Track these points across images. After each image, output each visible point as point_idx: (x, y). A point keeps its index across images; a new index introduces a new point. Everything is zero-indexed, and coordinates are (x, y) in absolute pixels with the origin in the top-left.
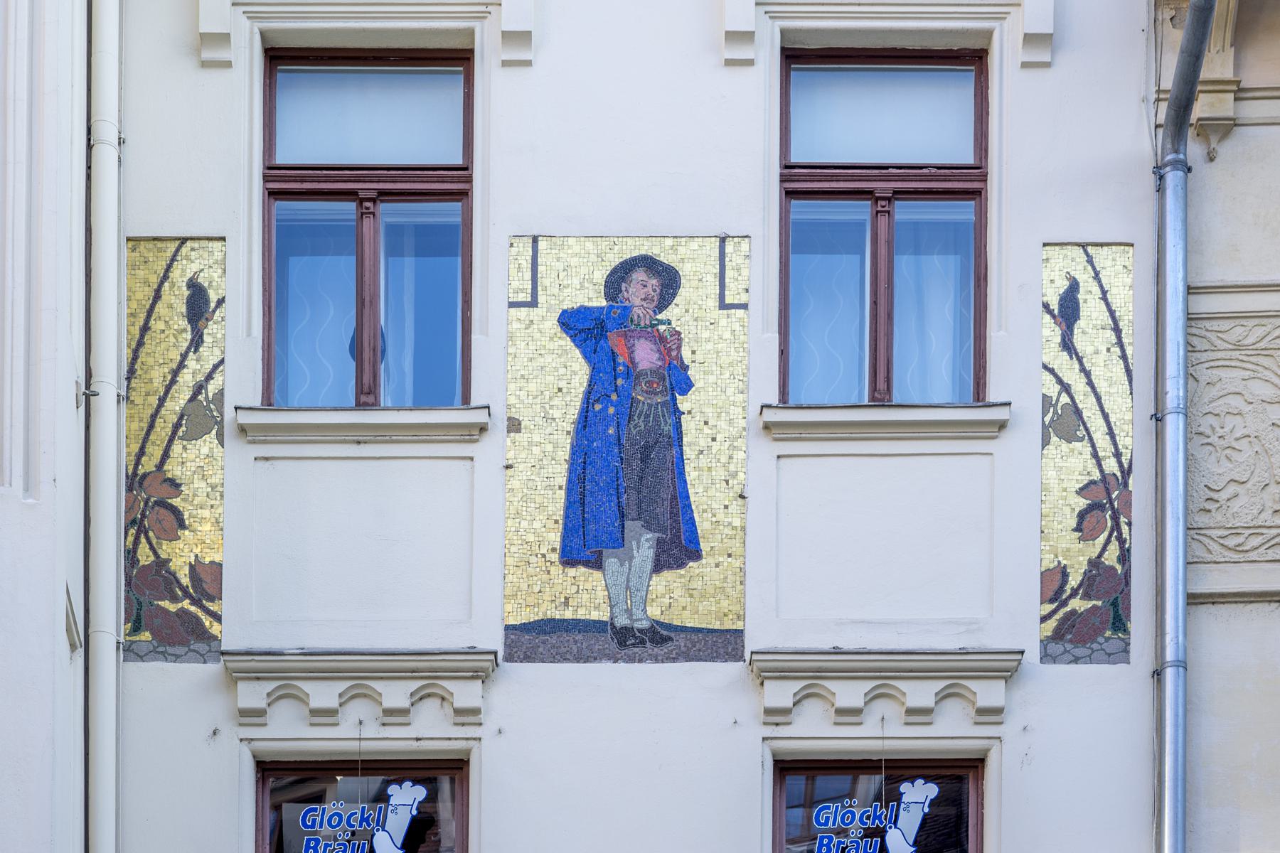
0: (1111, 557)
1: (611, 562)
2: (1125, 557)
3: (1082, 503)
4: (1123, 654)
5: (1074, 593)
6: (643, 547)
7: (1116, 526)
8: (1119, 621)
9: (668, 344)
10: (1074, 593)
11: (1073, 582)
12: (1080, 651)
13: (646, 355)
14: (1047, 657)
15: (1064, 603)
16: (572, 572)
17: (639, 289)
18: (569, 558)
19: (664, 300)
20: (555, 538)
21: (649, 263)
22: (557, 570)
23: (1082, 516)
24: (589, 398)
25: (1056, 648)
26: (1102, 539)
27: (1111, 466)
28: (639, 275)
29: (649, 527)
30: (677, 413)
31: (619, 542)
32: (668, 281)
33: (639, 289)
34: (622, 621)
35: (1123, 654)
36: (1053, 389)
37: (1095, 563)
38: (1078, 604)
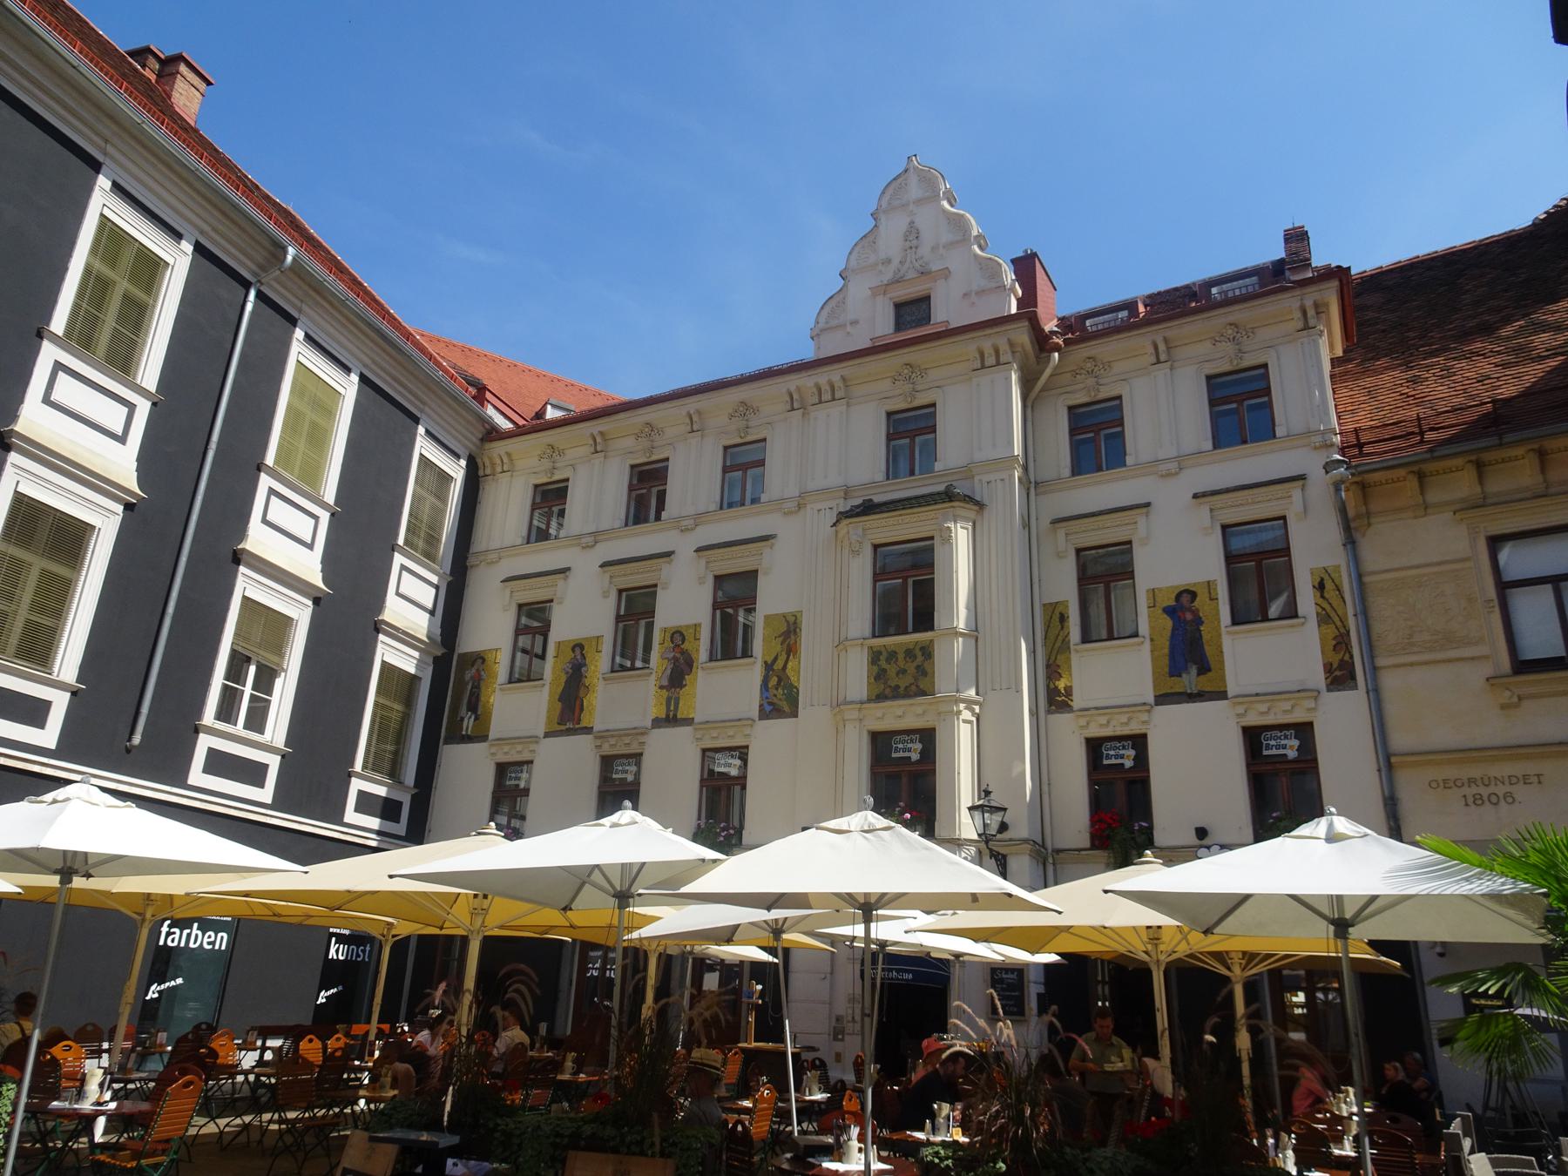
0: (1347, 657)
1: (1184, 675)
2: (1352, 657)
3: (1334, 642)
4: (1355, 687)
5: (1335, 670)
6: (1194, 671)
7: (1347, 647)
8: (1353, 677)
9: (1195, 613)
10: (1335, 670)
11: (1335, 666)
12: (1341, 687)
13: (1189, 616)
14: (1329, 690)
15: (1332, 673)
16: (1173, 678)
17: (1185, 599)
18: (1171, 675)
19: (1193, 601)
20: (1167, 670)
21: (1187, 591)
22: (1168, 679)
23: (1335, 646)
24: (1174, 629)
25: (1332, 687)
26: (1343, 653)
27: (1342, 630)
28: (1185, 595)
29: (1195, 664)
30: (1200, 631)
31: (1186, 669)
32: (1193, 595)
33: (1185, 599)
34: (1189, 691)
35: (1355, 687)
36: (1320, 610)
37: (1342, 660)
38: (1338, 673)
